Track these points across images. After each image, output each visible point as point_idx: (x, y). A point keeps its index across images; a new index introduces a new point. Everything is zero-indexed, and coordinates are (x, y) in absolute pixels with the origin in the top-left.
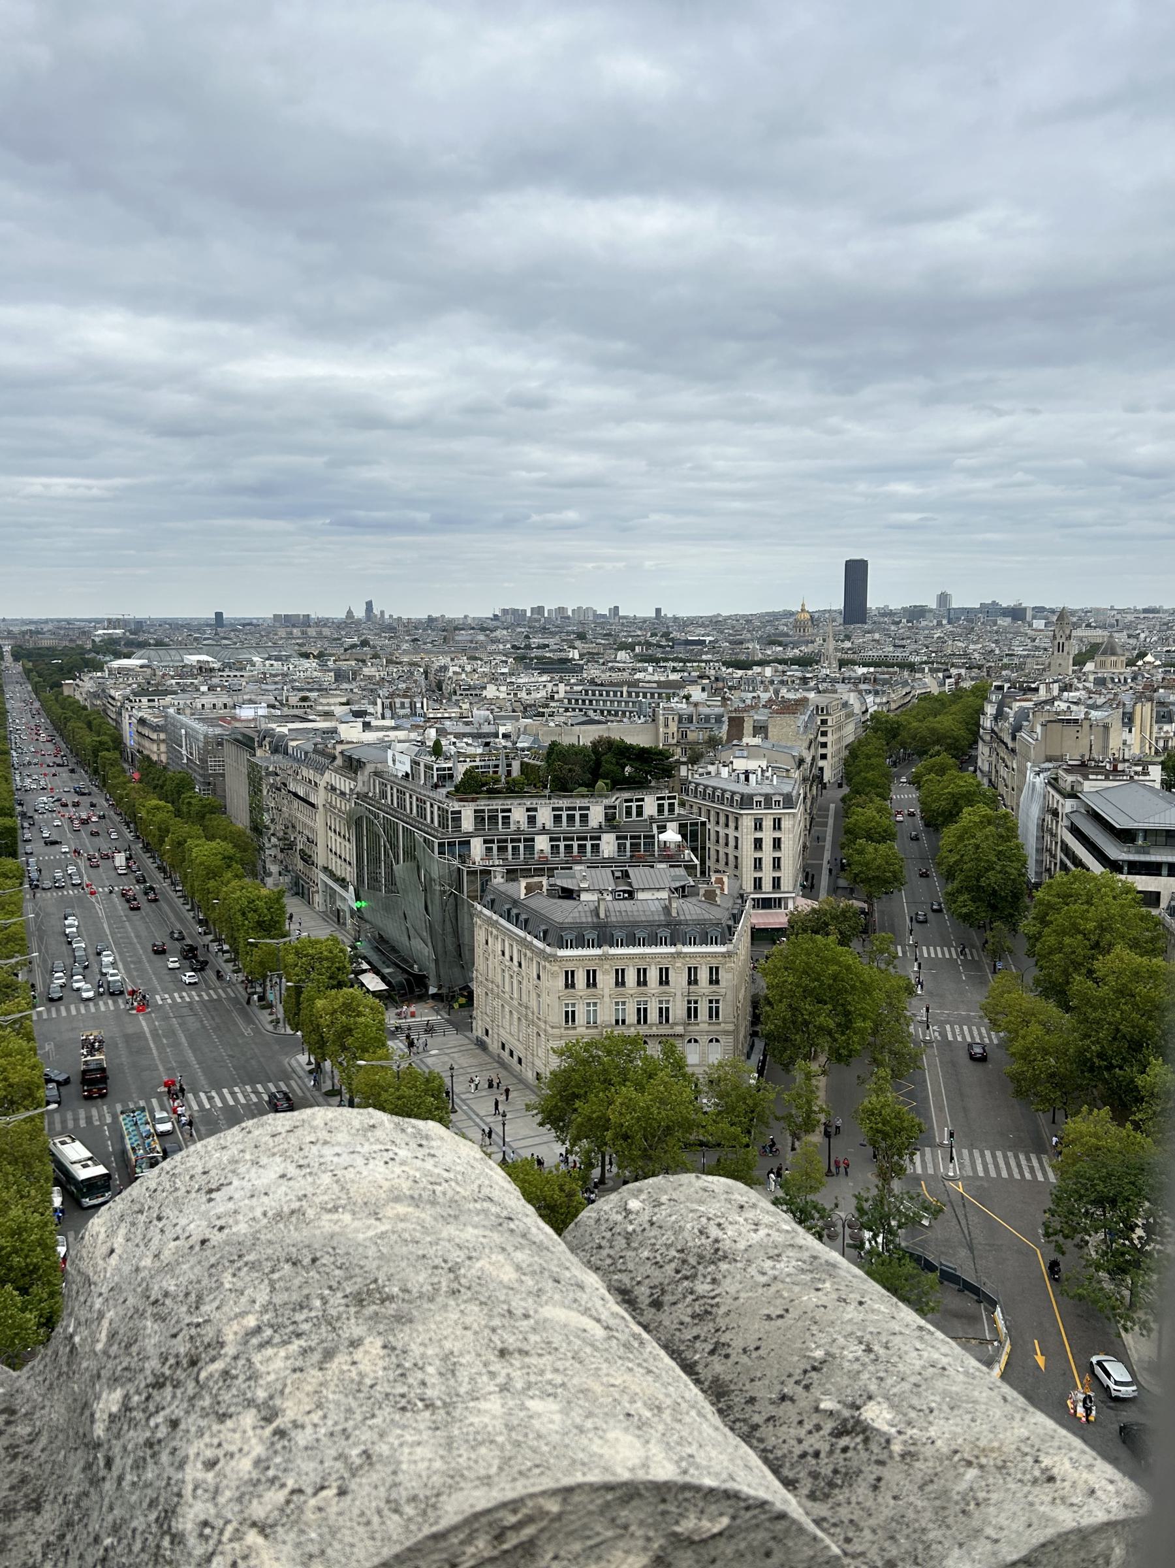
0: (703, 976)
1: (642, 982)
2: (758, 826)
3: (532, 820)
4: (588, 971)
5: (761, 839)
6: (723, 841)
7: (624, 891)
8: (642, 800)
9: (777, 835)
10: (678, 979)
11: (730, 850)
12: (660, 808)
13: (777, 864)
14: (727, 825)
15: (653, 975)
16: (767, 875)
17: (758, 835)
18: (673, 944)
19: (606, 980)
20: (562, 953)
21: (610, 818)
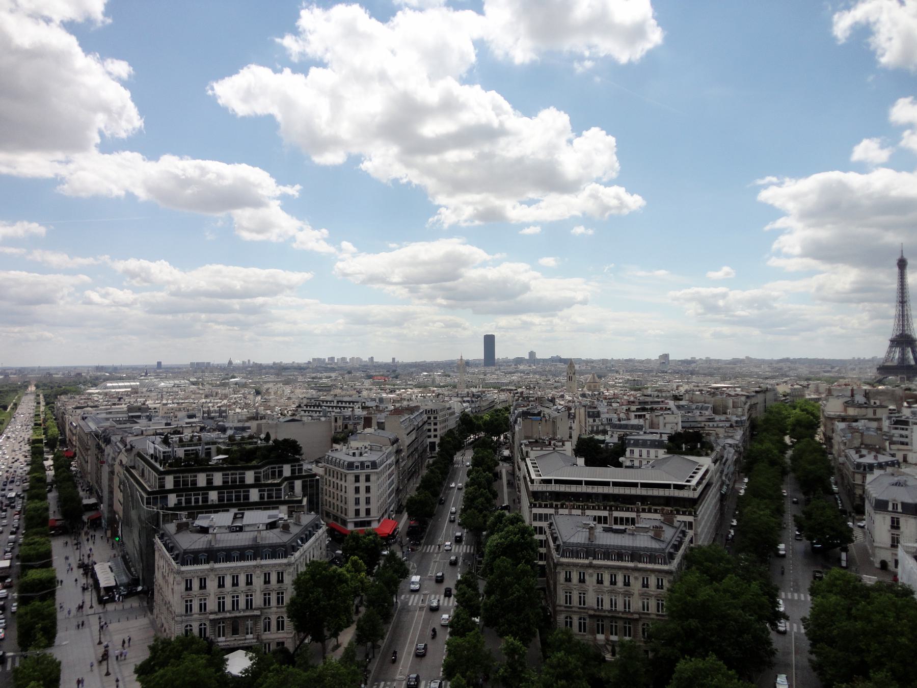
0: (274, 578)
1: (236, 584)
2: (357, 479)
3: (210, 481)
4: (201, 580)
5: (359, 487)
6: (339, 488)
7: (236, 527)
8: (282, 467)
9: (368, 484)
10: (258, 582)
11: (343, 493)
12: (293, 471)
13: (368, 501)
14: (341, 479)
15: (242, 579)
16: (363, 507)
17: (357, 485)
18: (255, 559)
19: (212, 585)
20: (184, 568)
21: (257, 479)
